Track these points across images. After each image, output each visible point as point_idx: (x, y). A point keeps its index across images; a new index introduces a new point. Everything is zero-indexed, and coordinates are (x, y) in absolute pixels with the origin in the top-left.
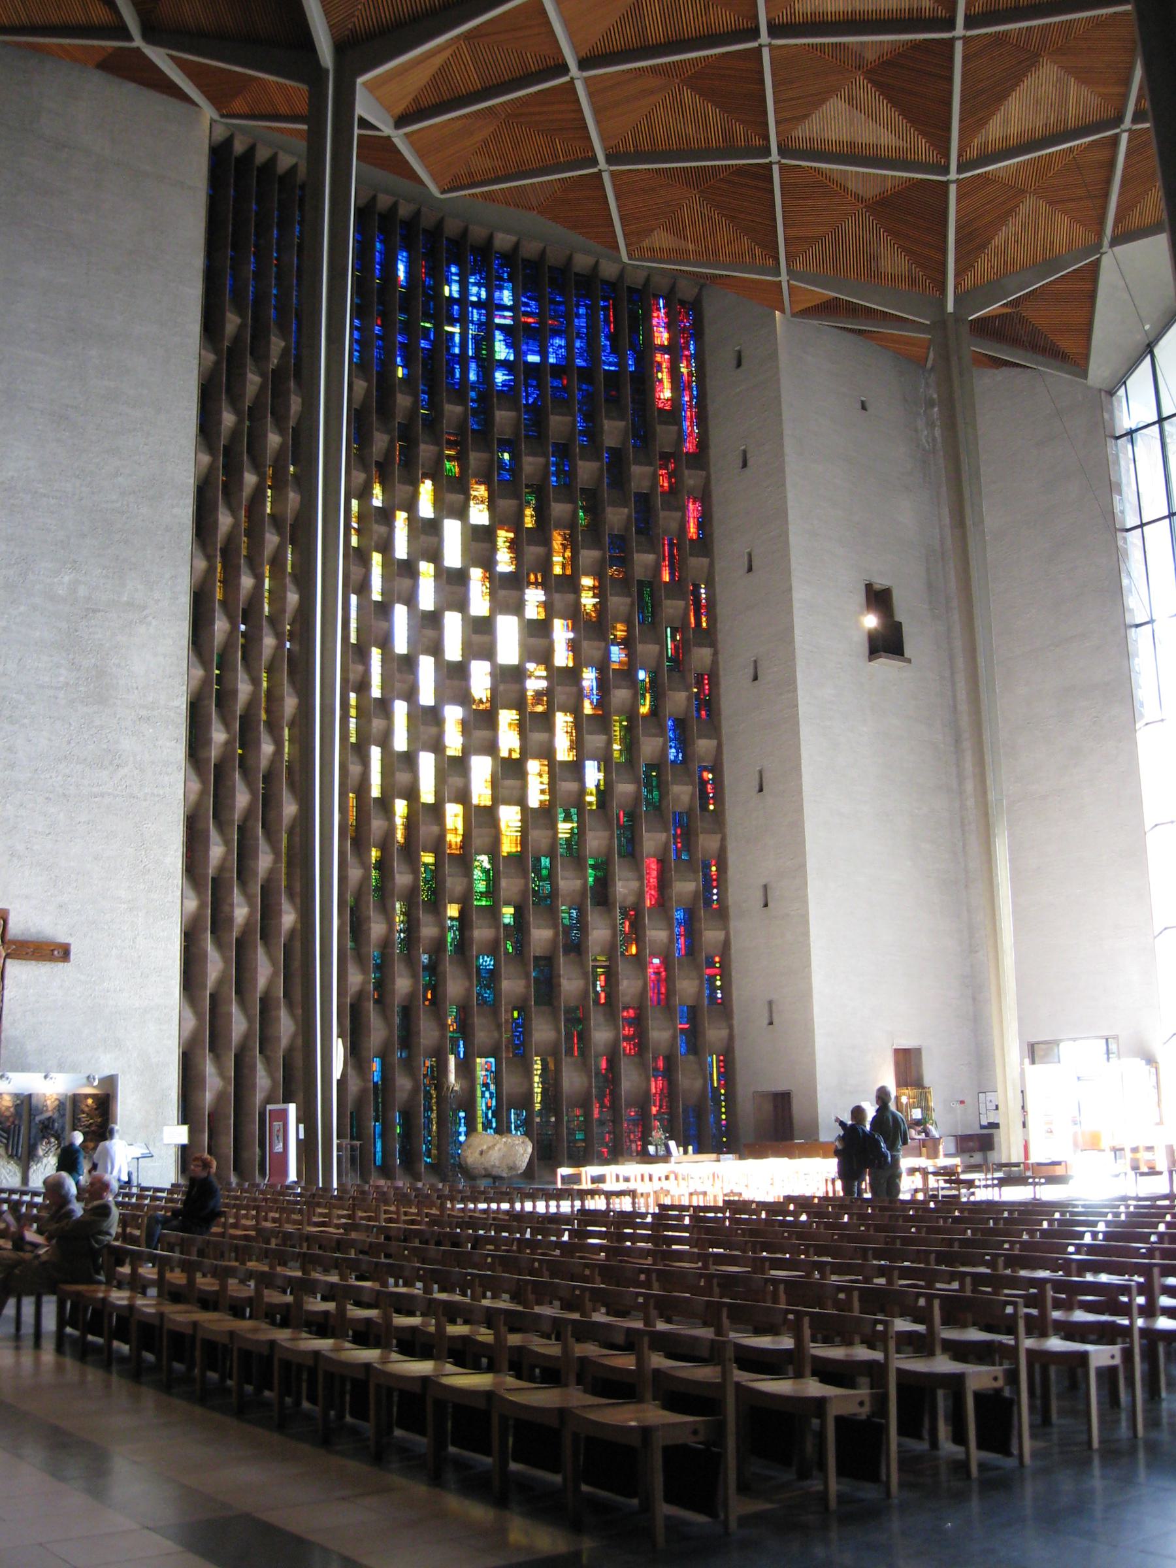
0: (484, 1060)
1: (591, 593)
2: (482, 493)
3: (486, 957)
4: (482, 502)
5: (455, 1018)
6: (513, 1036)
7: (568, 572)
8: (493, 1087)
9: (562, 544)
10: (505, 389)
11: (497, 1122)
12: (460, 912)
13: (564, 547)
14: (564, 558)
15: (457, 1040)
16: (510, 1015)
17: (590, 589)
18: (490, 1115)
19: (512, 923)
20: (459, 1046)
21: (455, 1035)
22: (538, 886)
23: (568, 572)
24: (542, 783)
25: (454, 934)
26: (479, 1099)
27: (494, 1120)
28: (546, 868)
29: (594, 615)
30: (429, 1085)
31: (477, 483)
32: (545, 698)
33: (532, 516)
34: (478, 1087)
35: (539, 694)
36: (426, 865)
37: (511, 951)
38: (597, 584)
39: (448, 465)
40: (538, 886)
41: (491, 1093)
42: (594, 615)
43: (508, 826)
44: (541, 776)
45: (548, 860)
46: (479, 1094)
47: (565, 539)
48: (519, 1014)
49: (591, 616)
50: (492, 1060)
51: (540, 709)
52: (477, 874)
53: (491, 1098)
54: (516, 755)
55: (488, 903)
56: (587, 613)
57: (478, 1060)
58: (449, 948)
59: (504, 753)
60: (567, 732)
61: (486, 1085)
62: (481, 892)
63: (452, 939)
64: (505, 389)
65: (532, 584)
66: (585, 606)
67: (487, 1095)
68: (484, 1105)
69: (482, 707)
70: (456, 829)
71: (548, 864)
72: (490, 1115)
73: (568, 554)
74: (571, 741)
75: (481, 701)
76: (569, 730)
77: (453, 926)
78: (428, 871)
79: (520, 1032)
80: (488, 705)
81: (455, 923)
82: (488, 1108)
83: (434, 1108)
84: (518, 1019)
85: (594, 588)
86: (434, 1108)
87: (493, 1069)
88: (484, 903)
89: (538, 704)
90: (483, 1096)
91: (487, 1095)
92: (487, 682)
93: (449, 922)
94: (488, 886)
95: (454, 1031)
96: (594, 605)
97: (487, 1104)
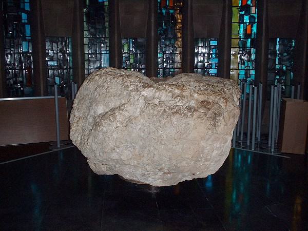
8: (254, 10)
11: (256, 54)
18: (249, 44)
26: (235, 26)
27: (253, 50)
30: (172, 8)
34: (235, 10)
41: (252, 18)
46: (235, 19)
53: (251, 23)
61: (246, 8)
67: (247, 19)
68: (241, 32)
72: (249, 44)
82: (247, 36)
83: (179, 35)
86: (179, 35)
90: (241, 21)
91: (247, 19)
97: (245, 30)
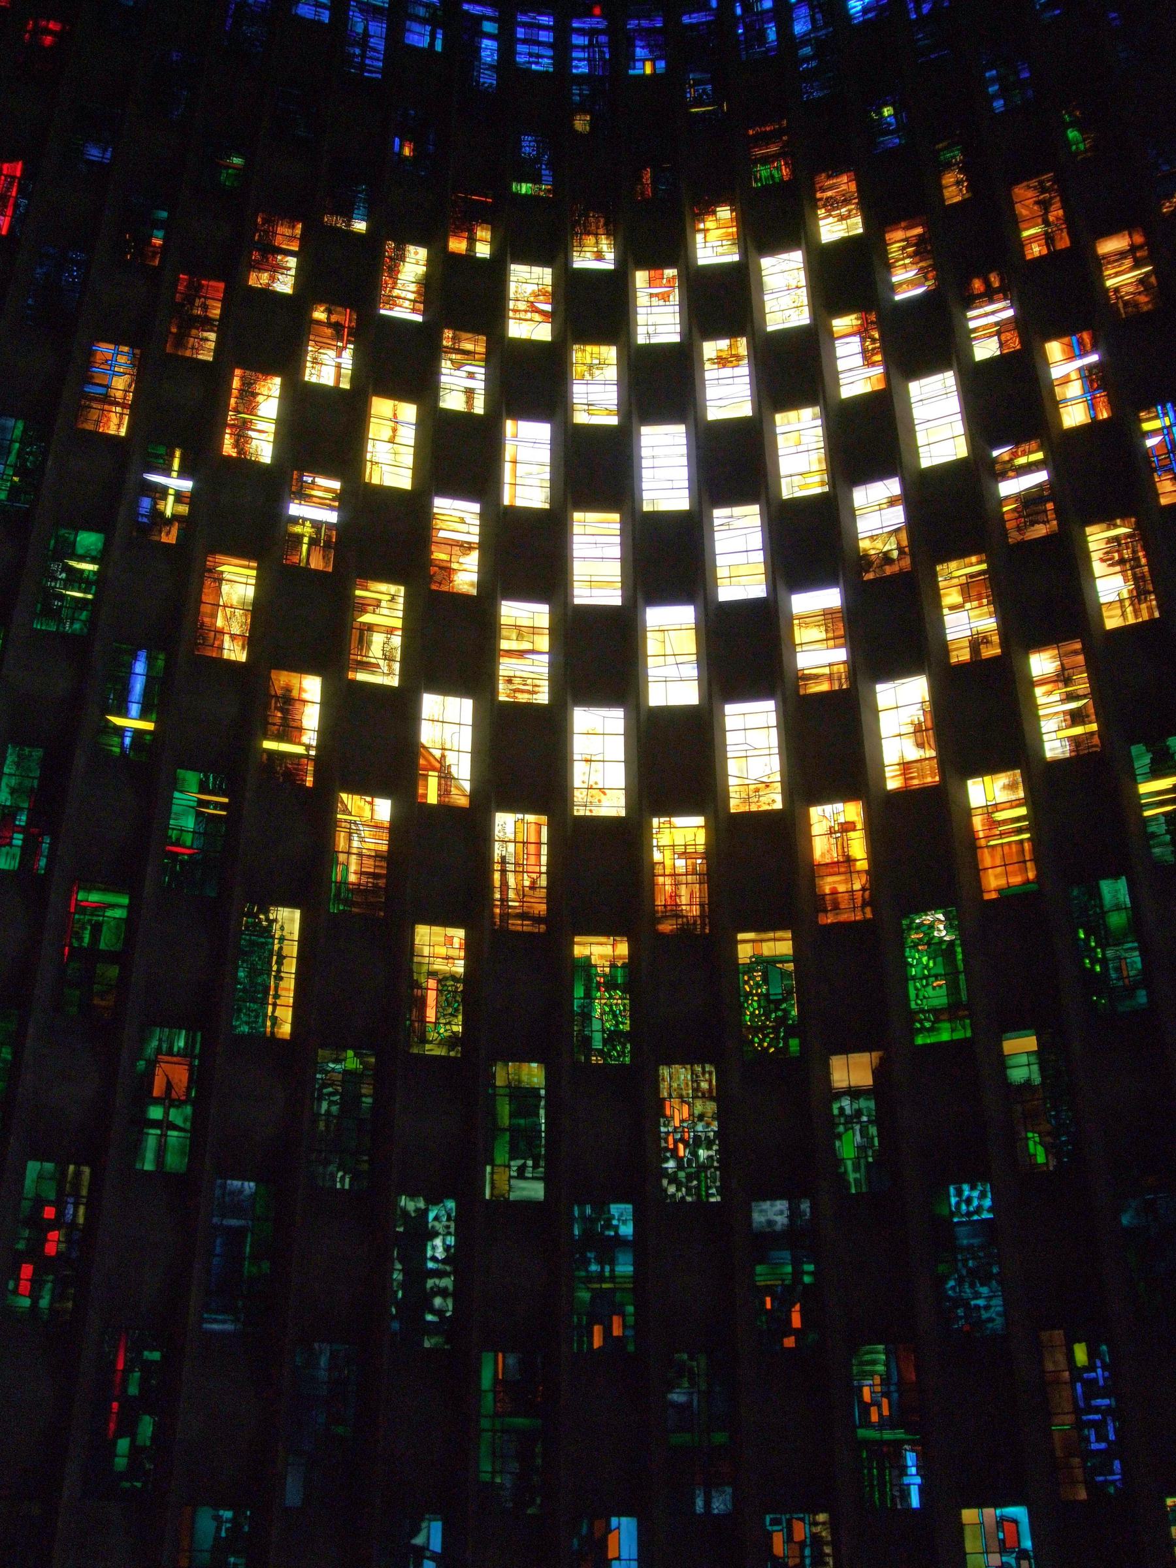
0: (991, 1514)
1: (1128, 263)
2: (844, 187)
3: (966, 1187)
4: (846, 202)
5: (886, 1381)
6: (1080, 1425)
7: (1063, 242)
9: (1037, 203)
10: (870, 16)
12: (878, 1073)
13: (1045, 205)
14: (1046, 222)
15: (898, 1445)
16: (1060, 1357)
17: (1122, 255)
19: (1037, 1079)
20: (903, 1471)
21: (888, 1435)
22: (1104, 962)
23: (1063, 242)
24: (1070, 697)
25: (864, 1133)
28: (1118, 908)
29: (1143, 299)
31: (829, 177)
32: (1050, 506)
33: (958, 183)
35: (1030, 502)
36: (766, 964)
37: (1041, 1159)
38: (1139, 239)
39: (763, 171)
40: (1104, 962)
42: (1143, 299)
43: (992, 824)
44: (1067, 681)
45: (1122, 885)
47: (1043, 190)
48: (1092, 1354)
49: (1136, 305)
50: (1018, 1512)
51: (1040, 531)
52: (919, 961)
54: (991, 651)
55: (960, 1035)
56: (1126, 304)
57: (969, 1515)
58: (852, 1176)
59: (961, 655)
60: (1122, 561)
62: (934, 1011)
63: (861, 1149)
64: (870, 16)
65: (980, 296)
66: (1117, 290)
69: (889, 570)
70: (849, 860)
71: (1124, 897)
73: (1056, 213)
74: (1136, 579)
75: (886, 558)
76: (1127, 554)
77: (859, 1113)
78: (774, 976)
79: (1108, 1411)
80: (906, 562)
81: (863, 1103)
84: (1091, 1367)
85: (1133, 249)
87: (1027, 1544)
88: (945, 1037)
89: (1033, 524)
92: (897, 516)
93: (846, 1103)
94: (953, 988)
95: (883, 1424)
96: (1141, 281)
